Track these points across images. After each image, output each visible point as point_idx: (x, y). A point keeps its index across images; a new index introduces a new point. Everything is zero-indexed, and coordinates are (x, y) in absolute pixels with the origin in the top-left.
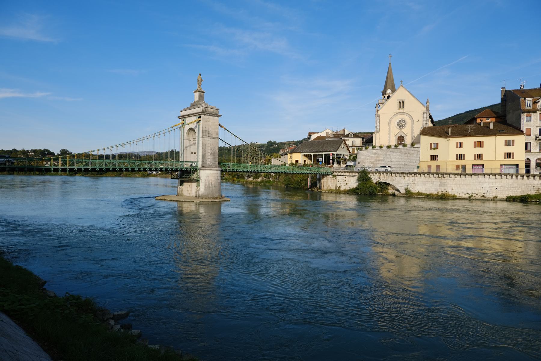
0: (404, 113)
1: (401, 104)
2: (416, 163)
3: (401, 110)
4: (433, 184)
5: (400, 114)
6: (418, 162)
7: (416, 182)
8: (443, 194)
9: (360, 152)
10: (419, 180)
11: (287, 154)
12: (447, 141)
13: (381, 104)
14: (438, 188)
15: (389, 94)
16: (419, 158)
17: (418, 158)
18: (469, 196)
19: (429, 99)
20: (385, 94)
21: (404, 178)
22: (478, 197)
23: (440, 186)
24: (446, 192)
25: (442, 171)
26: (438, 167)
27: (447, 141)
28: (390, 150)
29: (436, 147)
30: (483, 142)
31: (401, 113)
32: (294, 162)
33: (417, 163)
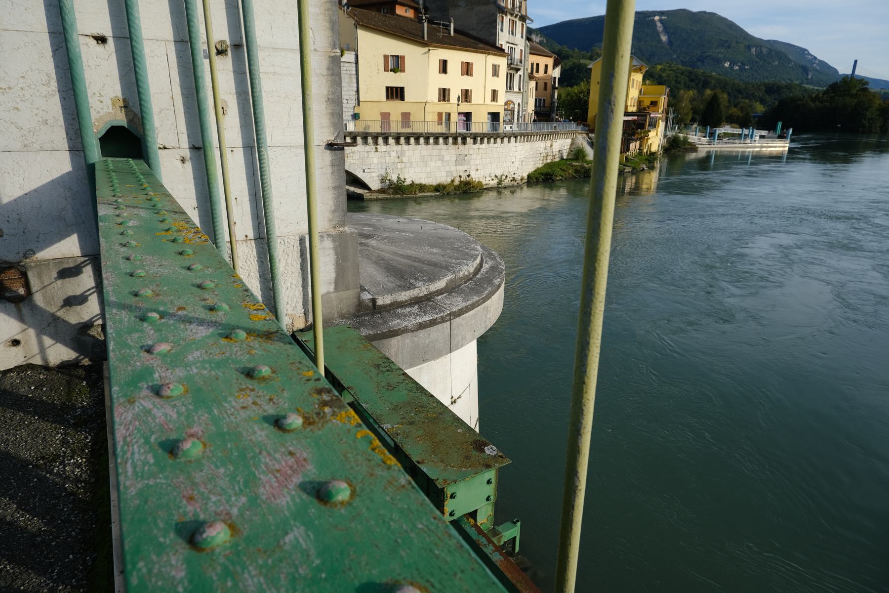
4: (443, 161)
6: (353, 103)
7: (405, 159)
10: (413, 152)
12: (425, 53)
14: (453, 169)
16: (354, 93)
17: (352, 91)
18: (497, 181)
21: (376, 148)
22: (507, 182)
23: (456, 165)
24: (468, 179)
25: (417, 128)
26: (406, 116)
27: (425, 53)
29: (396, 64)
30: (472, 64)
33: (352, 106)
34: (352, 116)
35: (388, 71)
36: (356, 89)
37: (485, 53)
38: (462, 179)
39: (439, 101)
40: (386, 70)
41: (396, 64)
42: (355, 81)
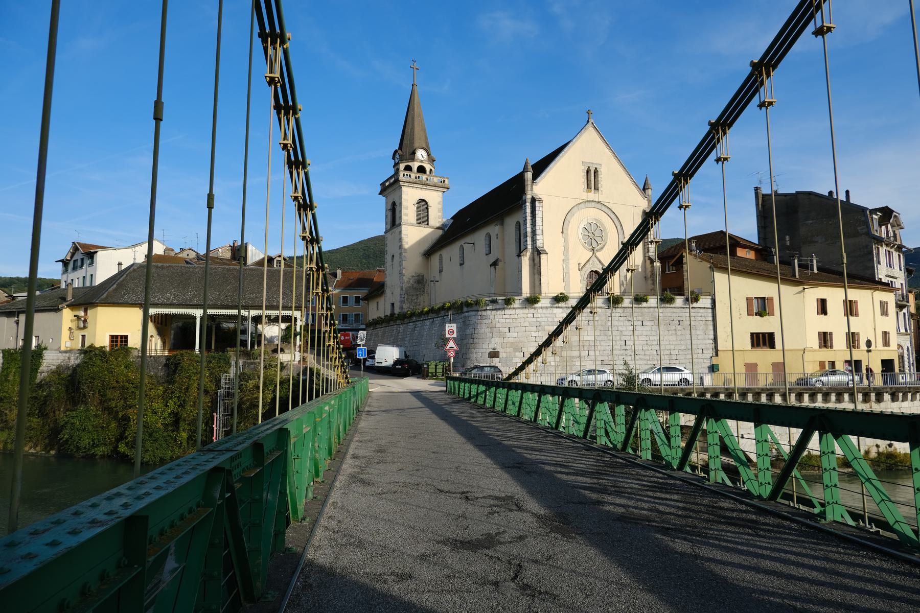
0: (599, 206)
1: (592, 177)
2: (705, 356)
3: (592, 196)
5: (587, 204)
6: (710, 352)
8: (882, 453)
9: (499, 312)
11: (57, 310)
12: (799, 292)
13: (406, 184)
15: (422, 161)
16: (711, 342)
17: (709, 339)
19: (649, 179)
20: (413, 160)
27: (799, 292)
28: (618, 310)
30: (856, 302)
31: (593, 204)
32: (102, 341)
33: (709, 356)
34: (708, 367)
35: (752, 315)
36: (712, 337)
37: (871, 289)
38: (881, 450)
39: (820, 347)
40: (750, 314)
41: (762, 307)
42: (711, 327)
